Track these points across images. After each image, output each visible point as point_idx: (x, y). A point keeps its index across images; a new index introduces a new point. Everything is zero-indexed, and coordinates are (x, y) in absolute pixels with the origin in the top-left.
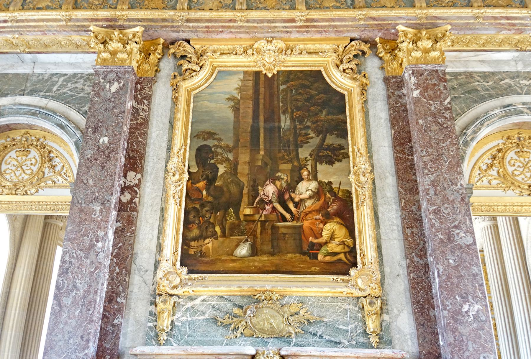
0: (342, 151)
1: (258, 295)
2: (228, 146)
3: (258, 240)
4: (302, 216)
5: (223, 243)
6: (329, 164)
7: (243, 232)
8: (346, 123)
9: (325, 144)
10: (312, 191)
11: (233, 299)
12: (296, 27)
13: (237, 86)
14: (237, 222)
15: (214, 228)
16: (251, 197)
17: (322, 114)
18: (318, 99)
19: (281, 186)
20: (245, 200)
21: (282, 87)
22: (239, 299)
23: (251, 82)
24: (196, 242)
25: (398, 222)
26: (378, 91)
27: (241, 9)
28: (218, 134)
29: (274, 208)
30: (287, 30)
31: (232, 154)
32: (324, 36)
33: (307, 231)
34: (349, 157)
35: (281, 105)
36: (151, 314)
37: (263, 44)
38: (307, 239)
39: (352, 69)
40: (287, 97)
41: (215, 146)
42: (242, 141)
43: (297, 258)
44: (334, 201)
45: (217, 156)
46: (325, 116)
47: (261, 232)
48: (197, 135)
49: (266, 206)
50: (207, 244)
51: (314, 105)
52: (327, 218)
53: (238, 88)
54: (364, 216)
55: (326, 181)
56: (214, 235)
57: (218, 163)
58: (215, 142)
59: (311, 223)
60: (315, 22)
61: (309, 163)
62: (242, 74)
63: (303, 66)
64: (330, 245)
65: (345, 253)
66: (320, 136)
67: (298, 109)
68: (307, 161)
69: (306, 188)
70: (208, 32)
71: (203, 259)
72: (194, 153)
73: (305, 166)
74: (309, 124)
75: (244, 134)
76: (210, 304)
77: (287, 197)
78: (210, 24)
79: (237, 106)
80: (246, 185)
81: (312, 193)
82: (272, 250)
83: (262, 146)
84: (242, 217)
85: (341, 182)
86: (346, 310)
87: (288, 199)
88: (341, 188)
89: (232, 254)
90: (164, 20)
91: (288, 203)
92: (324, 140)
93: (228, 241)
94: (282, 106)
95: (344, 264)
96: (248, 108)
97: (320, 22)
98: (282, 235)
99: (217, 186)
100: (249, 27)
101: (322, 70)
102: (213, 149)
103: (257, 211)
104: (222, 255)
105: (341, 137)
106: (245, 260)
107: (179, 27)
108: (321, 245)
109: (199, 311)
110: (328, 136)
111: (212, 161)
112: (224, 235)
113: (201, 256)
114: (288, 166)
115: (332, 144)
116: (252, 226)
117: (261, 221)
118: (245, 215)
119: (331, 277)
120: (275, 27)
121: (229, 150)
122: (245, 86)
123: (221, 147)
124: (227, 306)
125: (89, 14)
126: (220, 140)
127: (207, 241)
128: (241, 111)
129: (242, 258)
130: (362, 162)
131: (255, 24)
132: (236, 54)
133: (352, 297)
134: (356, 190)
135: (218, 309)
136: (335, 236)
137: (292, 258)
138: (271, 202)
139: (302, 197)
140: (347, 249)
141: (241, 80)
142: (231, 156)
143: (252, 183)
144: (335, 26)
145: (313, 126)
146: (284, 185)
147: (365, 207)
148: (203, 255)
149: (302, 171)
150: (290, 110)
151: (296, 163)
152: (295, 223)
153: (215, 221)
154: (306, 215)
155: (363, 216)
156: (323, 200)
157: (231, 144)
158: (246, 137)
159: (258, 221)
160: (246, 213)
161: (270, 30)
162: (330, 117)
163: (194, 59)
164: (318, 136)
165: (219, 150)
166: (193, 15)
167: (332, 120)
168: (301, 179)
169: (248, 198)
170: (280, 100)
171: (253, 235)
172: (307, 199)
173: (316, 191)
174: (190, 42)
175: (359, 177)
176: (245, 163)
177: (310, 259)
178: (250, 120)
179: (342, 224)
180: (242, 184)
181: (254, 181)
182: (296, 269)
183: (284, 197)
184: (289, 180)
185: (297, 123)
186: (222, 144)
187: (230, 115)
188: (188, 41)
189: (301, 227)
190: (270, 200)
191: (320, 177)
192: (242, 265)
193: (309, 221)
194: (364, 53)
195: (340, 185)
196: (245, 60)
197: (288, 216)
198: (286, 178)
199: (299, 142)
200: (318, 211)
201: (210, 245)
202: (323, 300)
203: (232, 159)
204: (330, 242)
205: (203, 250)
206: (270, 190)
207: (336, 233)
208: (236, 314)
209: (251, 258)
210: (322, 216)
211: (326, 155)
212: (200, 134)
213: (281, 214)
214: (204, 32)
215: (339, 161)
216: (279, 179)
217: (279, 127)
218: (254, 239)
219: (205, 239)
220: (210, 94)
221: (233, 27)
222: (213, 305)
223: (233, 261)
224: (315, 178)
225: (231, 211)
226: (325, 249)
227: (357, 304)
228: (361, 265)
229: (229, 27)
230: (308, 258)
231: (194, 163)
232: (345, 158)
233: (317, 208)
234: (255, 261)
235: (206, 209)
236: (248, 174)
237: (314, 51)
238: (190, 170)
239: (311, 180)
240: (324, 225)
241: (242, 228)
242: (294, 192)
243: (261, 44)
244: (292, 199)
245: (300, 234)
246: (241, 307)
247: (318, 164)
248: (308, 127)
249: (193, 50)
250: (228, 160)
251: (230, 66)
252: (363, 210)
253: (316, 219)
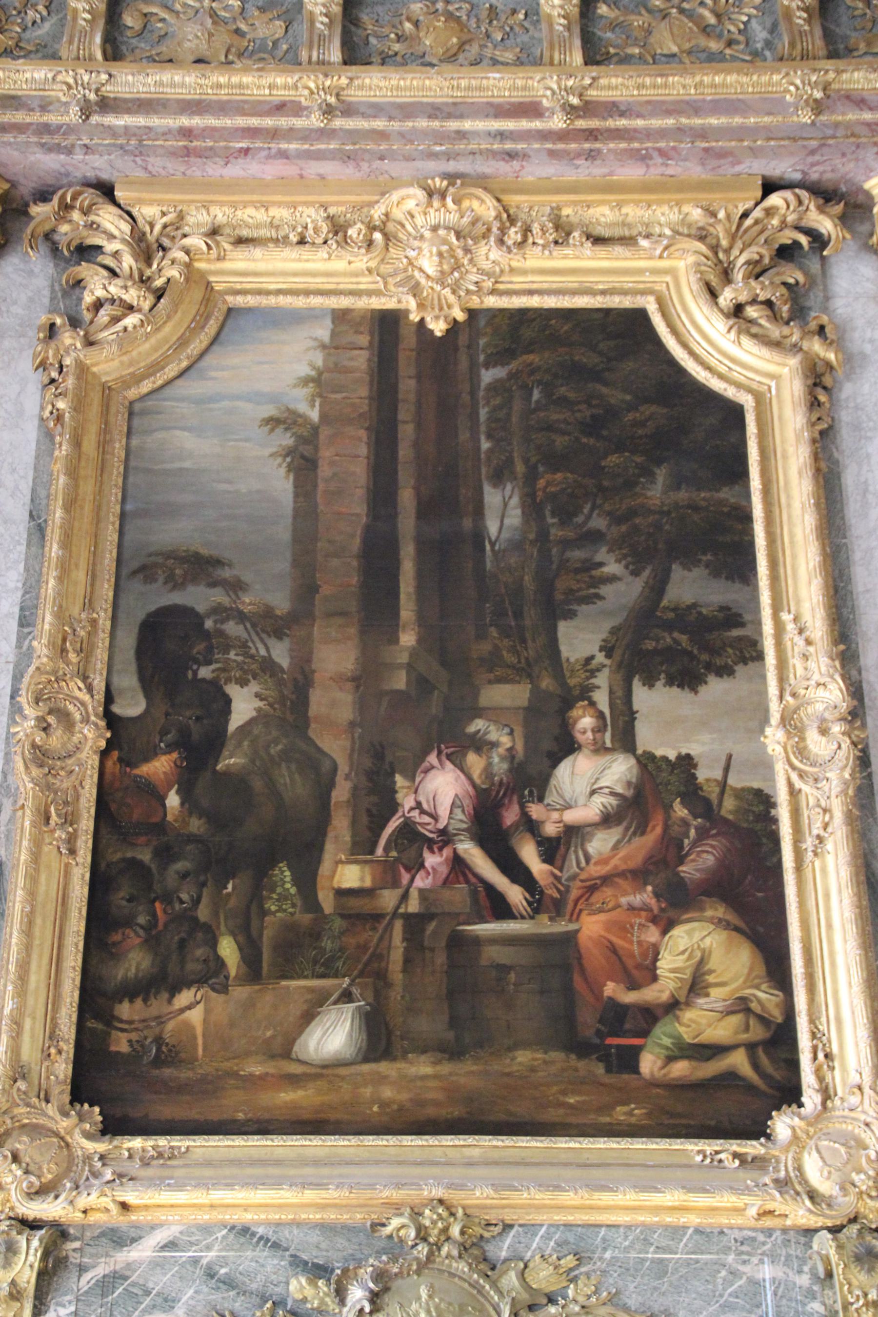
0: (736, 633)
1: (395, 1222)
2: (268, 613)
3: (396, 995)
4: (574, 893)
5: (249, 1005)
6: (681, 686)
7: (332, 959)
8: (747, 518)
9: (664, 603)
10: (613, 794)
11: (292, 1237)
12: (545, 136)
13: (305, 370)
14: (306, 918)
15: (213, 943)
16: (364, 820)
17: (653, 482)
18: (636, 424)
19: (488, 772)
20: (341, 827)
21: (488, 376)
22: (314, 1237)
23: (365, 354)
24: (139, 1002)
27: (321, 63)
28: (230, 565)
29: (458, 864)
30: (509, 146)
31: (286, 644)
32: (655, 171)
33: (594, 958)
34: (760, 657)
35: (485, 445)
37: (410, 204)
38: (597, 993)
39: (769, 303)
40: (509, 415)
41: (217, 610)
42: (326, 590)
43: (553, 1069)
44: (703, 834)
45: (226, 649)
46: (664, 492)
47: (407, 961)
48: (143, 568)
49: (426, 854)
50: (182, 1011)
51: (619, 448)
52: (678, 902)
53: (312, 380)
54: (827, 896)
55: (672, 755)
56: (212, 975)
57: (228, 680)
58: (218, 596)
59: (609, 926)
60: (622, 114)
61: (602, 680)
62: (328, 322)
63: (574, 293)
64: (688, 1015)
65: (751, 1047)
66: (646, 573)
67: (555, 461)
68: (593, 673)
69: (589, 783)
70: (188, 152)
71: (167, 1072)
72: (128, 640)
73: (585, 693)
74: (598, 523)
75: (335, 562)
76: (195, 1261)
77: (510, 816)
78: (196, 121)
79: (307, 450)
80: (343, 767)
81: (613, 801)
82: (451, 1035)
83: (407, 612)
84: (327, 901)
85: (730, 757)
86: (756, 1284)
87: (516, 826)
88: (732, 781)
89: (286, 1054)
91: (514, 842)
92: (658, 587)
93: (269, 997)
94: (490, 451)
95: (747, 1091)
96: (348, 461)
97: (639, 116)
98: (494, 973)
99: (227, 774)
100: (353, 135)
101: (652, 308)
102: (209, 624)
103: (388, 876)
104: (247, 1054)
105: (730, 578)
106: (343, 1078)
107: (70, 129)
108: (650, 1016)
109: (148, 1293)
110: (677, 572)
111: (205, 672)
112: (253, 971)
113: (159, 1062)
114: (509, 695)
115: (694, 605)
116: (370, 936)
117: (407, 917)
118: (342, 893)
119: (693, 1148)
120: (462, 135)
121: (271, 624)
122: (338, 369)
123: (241, 617)
126: (236, 586)
127: (185, 997)
128: (324, 471)
129: (328, 1070)
130: (816, 677)
131: (379, 124)
132: (302, 242)
133: (785, 1230)
134: (794, 793)
135: (229, 1283)
136: (711, 979)
137: (533, 1069)
138: (445, 838)
139: (571, 817)
140: (757, 1033)
141: (323, 347)
142: (281, 653)
143: (368, 763)
144: (702, 134)
145: (615, 531)
146: (500, 767)
147: (830, 859)
148: (168, 1054)
149: (575, 713)
150: (520, 468)
151: (546, 683)
152: (545, 926)
153: (216, 914)
154: (591, 889)
156: (659, 830)
157: (281, 602)
158: (342, 576)
159: (395, 914)
160: (346, 885)
161: (438, 148)
162: (683, 495)
163: (128, 261)
164: (635, 573)
165: (233, 628)
166: (130, 81)
167: (696, 508)
168: (567, 746)
169: (354, 822)
170: (483, 428)
171: (374, 974)
172: (595, 825)
173: (629, 793)
174: (118, 193)
175: (803, 739)
176: (339, 679)
177: (609, 1070)
178: (356, 506)
179: (737, 929)
180: (326, 766)
181: (378, 754)
182: (553, 1115)
183: (498, 820)
184: (520, 747)
185: (550, 520)
186: (248, 602)
187: (281, 485)
188: (107, 191)
189: (569, 939)
190: (443, 832)
191: (648, 738)
192: (326, 1098)
193: (602, 917)
194: (819, 241)
195: (727, 770)
196: (339, 265)
197: (515, 894)
198: (506, 741)
199: (559, 596)
200: (639, 876)
201: (195, 1016)
202: (664, 1243)
203: (285, 663)
204: (688, 1004)
205: (166, 1036)
206: (443, 789)
207: (711, 965)
208: (305, 1300)
209: (366, 1068)
210: (657, 895)
211: (669, 648)
212: (155, 565)
213: (490, 888)
214: (173, 154)
215: (725, 671)
216: (480, 744)
217: (479, 537)
218: (377, 994)
219: (174, 990)
220: (200, 401)
221: (290, 134)
222: (209, 1267)
223: (294, 1080)
224: (626, 740)
225: (284, 875)
226: (668, 1029)
227: (803, 1261)
228: (818, 1098)
229: (274, 134)
230: (600, 1069)
231: (128, 681)
232: (744, 661)
233: (636, 862)
234: (382, 1079)
235: (181, 866)
236: (352, 724)
237: (618, 232)
238: (116, 709)
239: (607, 750)
240: (665, 932)
241: (327, 944)
242: (541, 799)
243: (406, 202)
244: (532, 827)
245: (566, 969)
247: (637, 684)
248: (595, 537)
249: (126, 228)
250: (268, 666)
251: (279, 292)
252: (824, 870)
253: (631, 908)
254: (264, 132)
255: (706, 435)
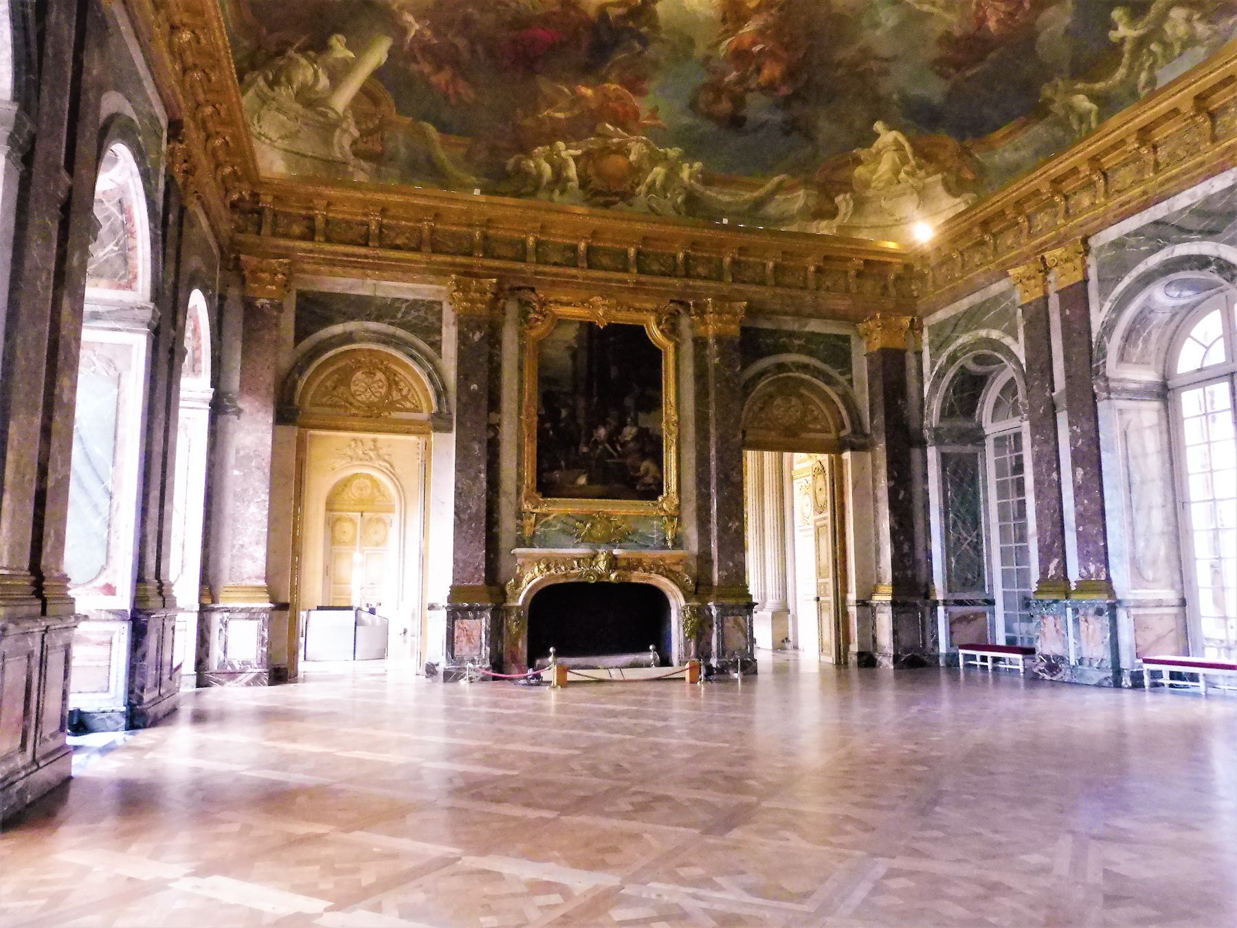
20: (583, 439)
25: (693, 462)
26: (688, 348)
36: (518, 525)
52: (644, 456)
56: (559, 468)
69: (629, 432)
90: (514, 271)
96: (583, 357)
103: (591, 450)
112: (567, 468)
114: (614, 413)
124: (571, 521)
125: (449, 259)
138: (602, 443)
142: (570, 402)
155: (670, 458)
166: (541, 268)
168: (625, 424)
187: (570, 363)
206: (602, 432)
246: (581, 522)
254: (569, 283)
255: (655, 355)
